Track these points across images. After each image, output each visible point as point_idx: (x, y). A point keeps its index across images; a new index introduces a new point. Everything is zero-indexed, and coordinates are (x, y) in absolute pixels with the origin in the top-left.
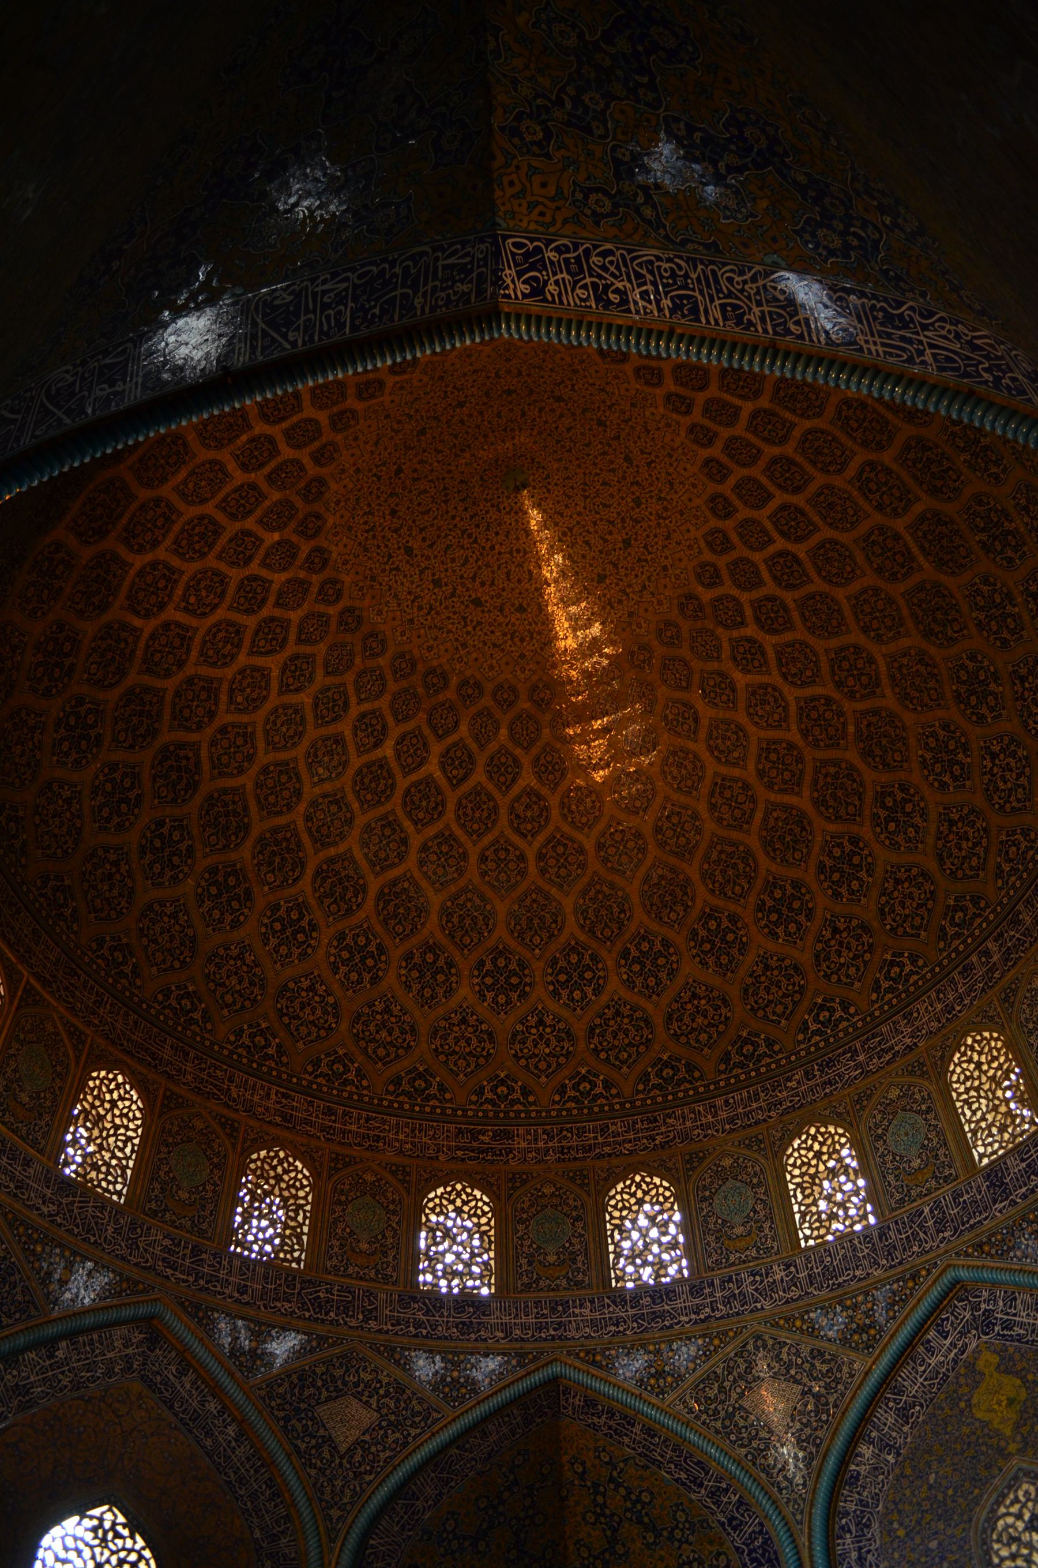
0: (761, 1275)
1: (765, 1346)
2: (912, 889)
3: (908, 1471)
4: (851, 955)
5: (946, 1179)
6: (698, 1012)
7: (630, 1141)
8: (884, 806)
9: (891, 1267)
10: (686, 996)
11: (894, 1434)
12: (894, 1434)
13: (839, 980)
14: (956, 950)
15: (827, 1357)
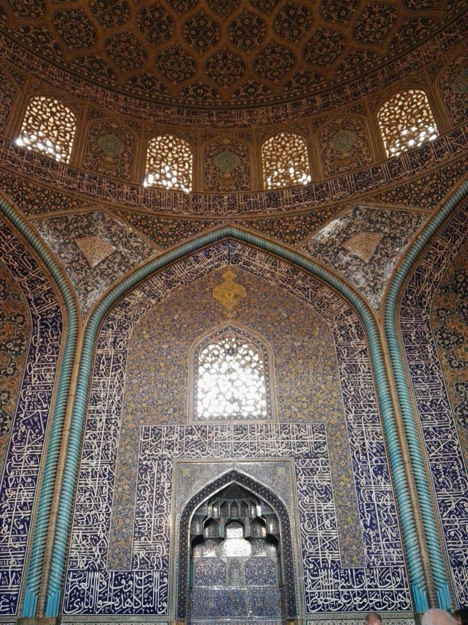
0: (115, 186)
1: (103, 219)
2: (280, 58)
3: (162, 310)
4: (229, 72)
5: (242, 188)
6: (127, 50)
7: (59, 82)
8: (287, 13)
9: (195, 214)
10: (123, 38)
11: (160, 291)
12: (160, 291)
13: (216, 80)
14: (295, 94)
15: (139, 240)
